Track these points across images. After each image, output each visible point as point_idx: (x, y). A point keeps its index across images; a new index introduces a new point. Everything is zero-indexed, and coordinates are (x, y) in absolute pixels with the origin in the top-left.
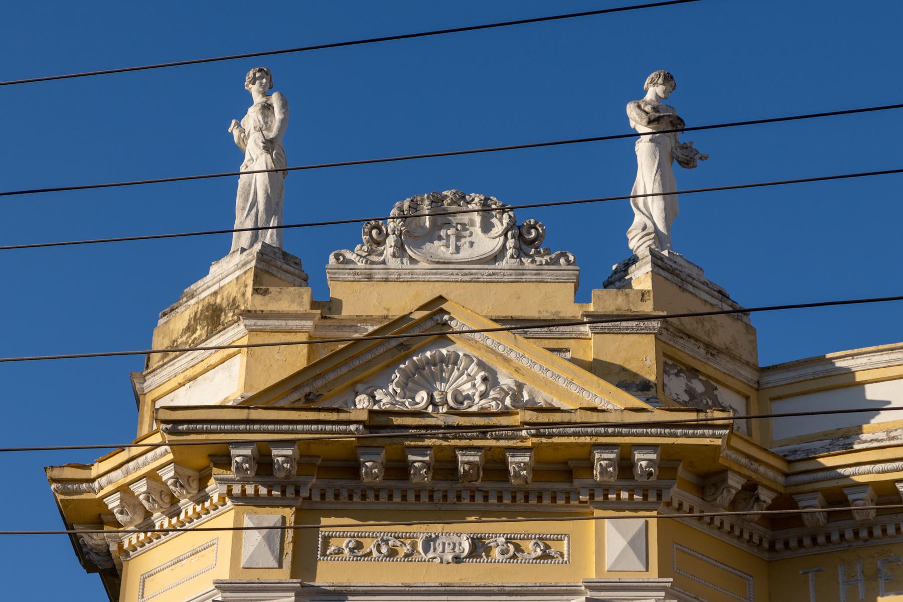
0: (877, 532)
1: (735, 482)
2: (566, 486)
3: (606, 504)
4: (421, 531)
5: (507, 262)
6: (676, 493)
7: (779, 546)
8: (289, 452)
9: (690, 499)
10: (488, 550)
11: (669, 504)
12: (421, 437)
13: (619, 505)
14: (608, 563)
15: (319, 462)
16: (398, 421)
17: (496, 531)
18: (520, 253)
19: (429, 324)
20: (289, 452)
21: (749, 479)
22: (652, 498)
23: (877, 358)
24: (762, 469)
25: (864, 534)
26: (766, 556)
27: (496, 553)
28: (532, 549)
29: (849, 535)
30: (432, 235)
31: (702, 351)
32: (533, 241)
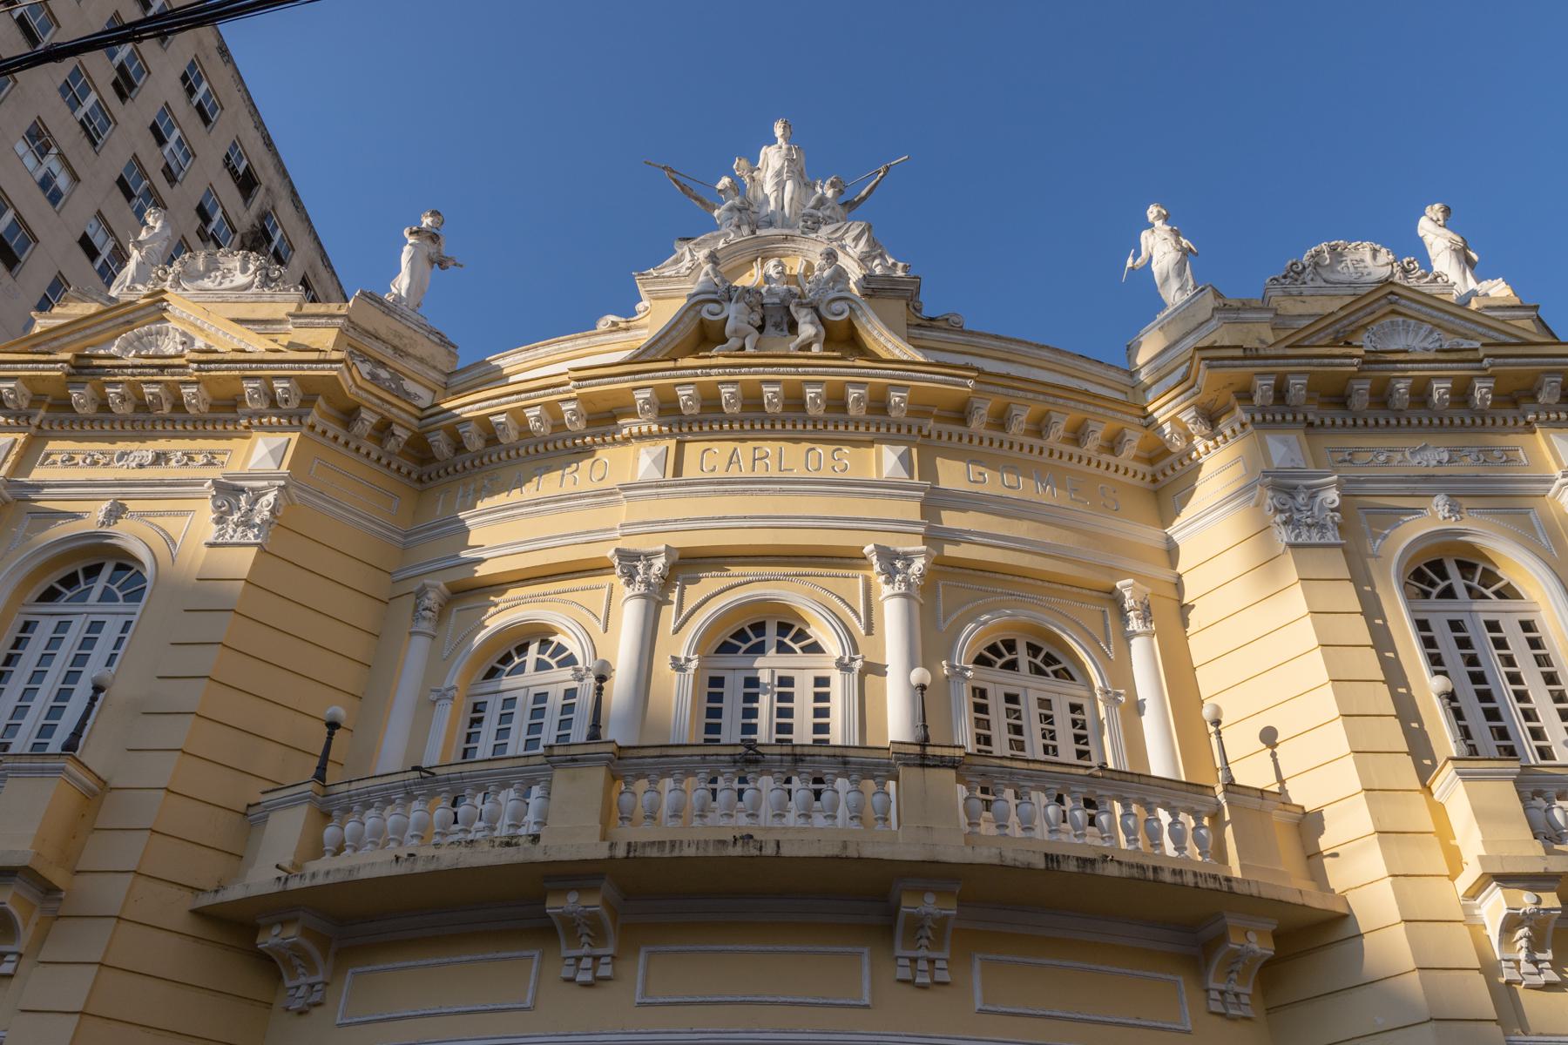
0: (486, 460)
1: (369, 418)
2: (233, 416)
3: (261, 427)
4: (120, 446)
5: (254, 290)
6: (314, 417)
7: (425, 478)
8: (12, 385)
9: (334, 429)
10: (168, 461)
11: (312, 427)
12: (115, 375)
13: (271, 429)
14: (251, 464)
15: (49, 400)
16: (96, 362)
17: (177, 446)
18: (264, 284)
19: (153, 309)
20: (12, 385)
21: (383, 417)
22: (295, 422)
23: (519, 357)
24: (394, 410)
25: (477, 462)
26: (417, 486)
27: (173, 463)
28: (200, 459)
29: (468, 464)
30: (206, 274)
31: (390, 351)
32: (274, 280)
